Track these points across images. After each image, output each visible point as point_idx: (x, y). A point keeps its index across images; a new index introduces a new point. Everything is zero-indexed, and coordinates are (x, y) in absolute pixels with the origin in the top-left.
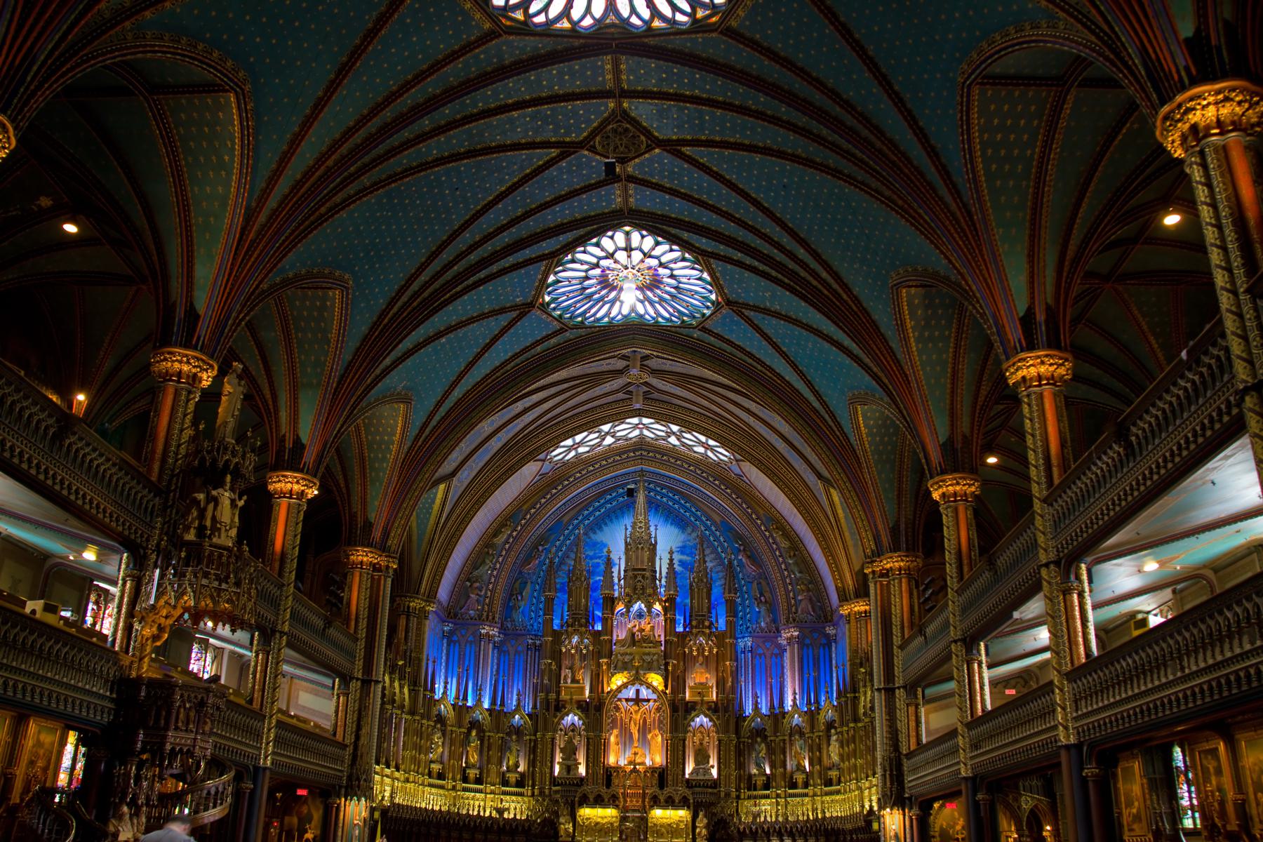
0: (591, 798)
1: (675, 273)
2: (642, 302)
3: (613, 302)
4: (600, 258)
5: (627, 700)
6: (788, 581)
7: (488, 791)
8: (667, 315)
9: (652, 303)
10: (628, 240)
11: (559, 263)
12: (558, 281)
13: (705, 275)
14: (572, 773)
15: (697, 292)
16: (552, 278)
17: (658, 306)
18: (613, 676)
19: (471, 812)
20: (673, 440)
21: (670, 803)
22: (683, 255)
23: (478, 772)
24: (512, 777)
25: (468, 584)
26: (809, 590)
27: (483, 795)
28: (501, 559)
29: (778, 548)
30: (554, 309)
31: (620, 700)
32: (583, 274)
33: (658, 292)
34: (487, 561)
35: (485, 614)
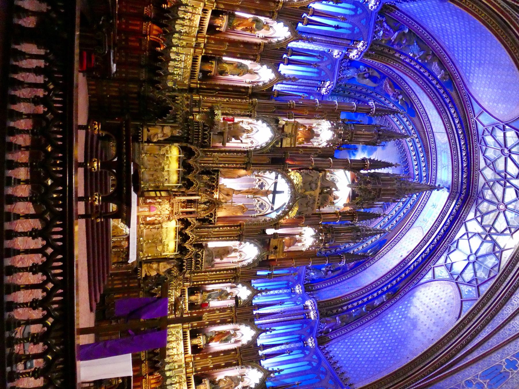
0: (191, 162)
5: (276, 184)
6: (350, 306)
7: (200, 40)
14: (215, 137)
18: (301, 174)
19: (179, 21)
20: (473, 226)
21: (182, 236)
23: (223, 29)
24: (212, 67)
25: (407, 31)
26: (342, 322)
27: (195, 33)
28: (417, 67)
29: (374, 299)
31: (276, 178)
34: (421, 54)
35: (375, 47)
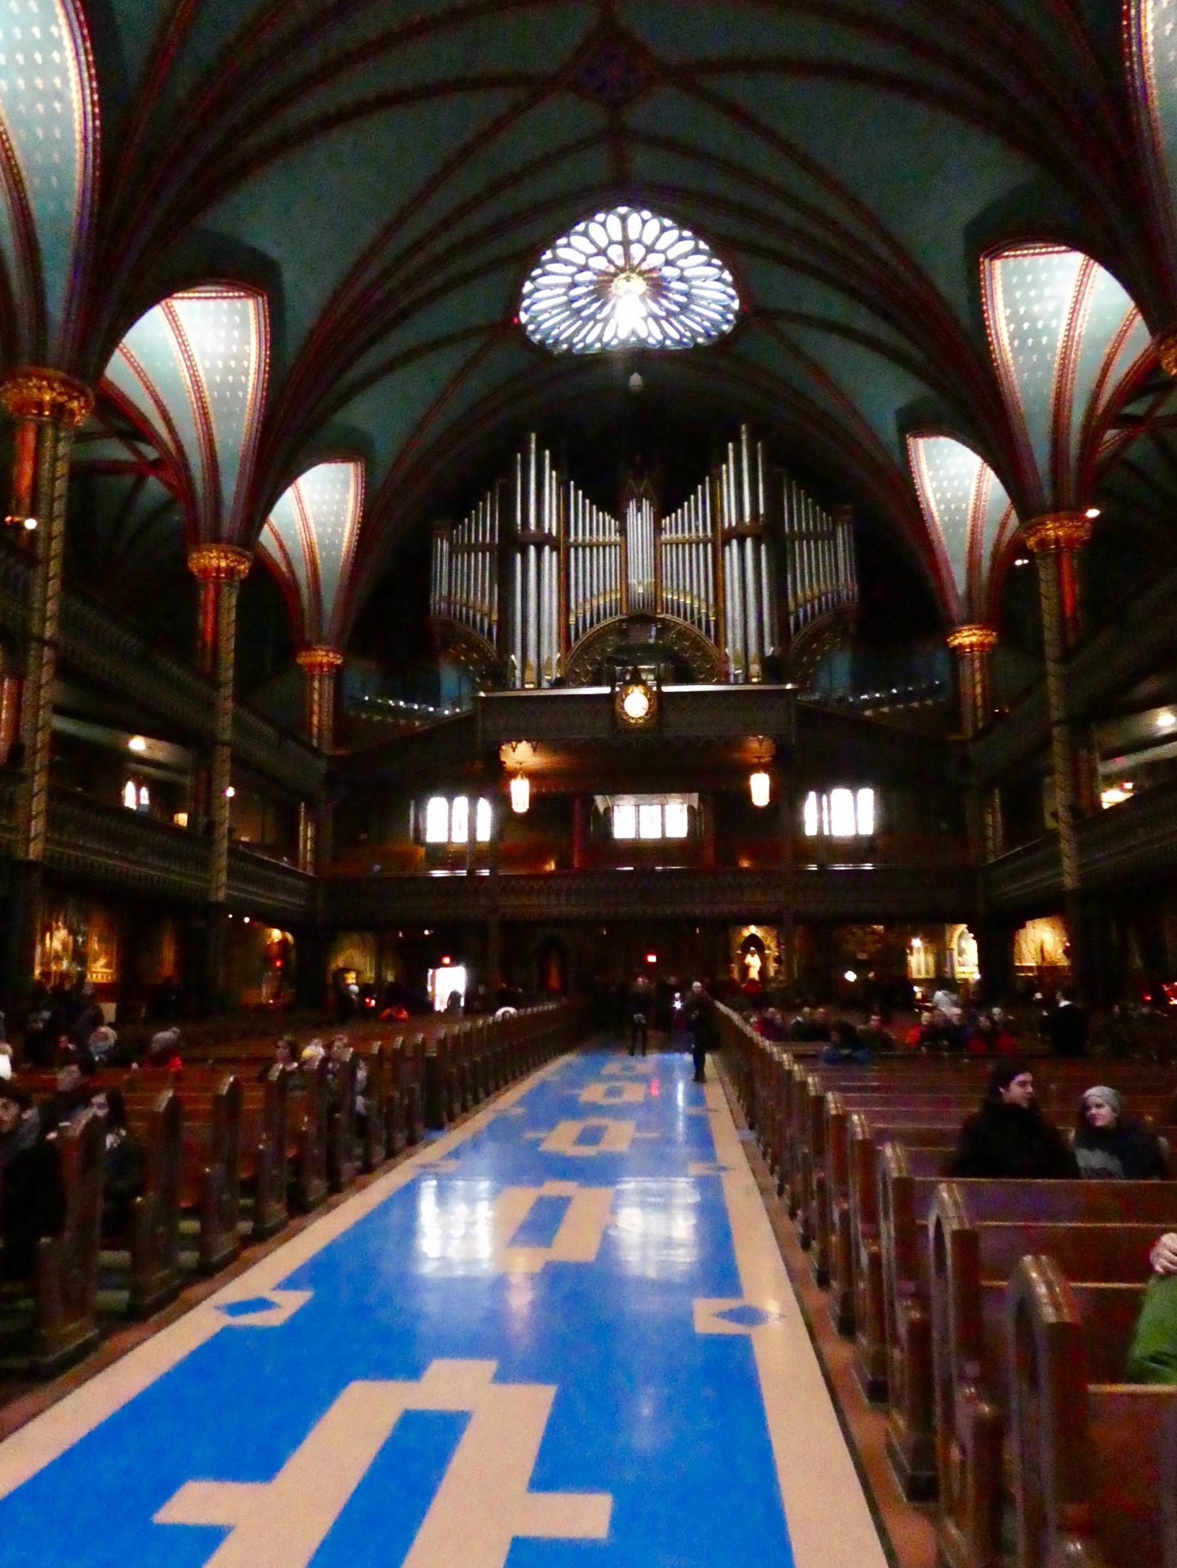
1: (687, 273)
2: (645, 320)
3: (606, 320)
4: (588, 256)
8: (677, 336)
9: (656, 318)
10: (624, 229)
11: (539, 264)
12: (537, 290)
13: (727, 276)
15: (715, 301)
16: (528, 287)
17: (663, 322)
22: (697, 245)
30: (534, 332)
32: (569, 280)
33: (664, 302)
